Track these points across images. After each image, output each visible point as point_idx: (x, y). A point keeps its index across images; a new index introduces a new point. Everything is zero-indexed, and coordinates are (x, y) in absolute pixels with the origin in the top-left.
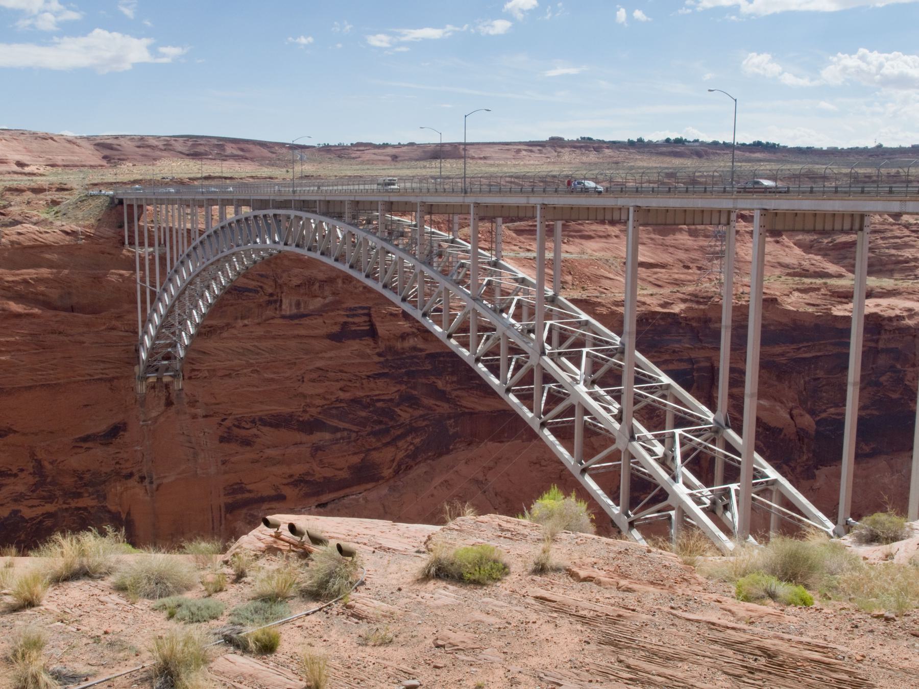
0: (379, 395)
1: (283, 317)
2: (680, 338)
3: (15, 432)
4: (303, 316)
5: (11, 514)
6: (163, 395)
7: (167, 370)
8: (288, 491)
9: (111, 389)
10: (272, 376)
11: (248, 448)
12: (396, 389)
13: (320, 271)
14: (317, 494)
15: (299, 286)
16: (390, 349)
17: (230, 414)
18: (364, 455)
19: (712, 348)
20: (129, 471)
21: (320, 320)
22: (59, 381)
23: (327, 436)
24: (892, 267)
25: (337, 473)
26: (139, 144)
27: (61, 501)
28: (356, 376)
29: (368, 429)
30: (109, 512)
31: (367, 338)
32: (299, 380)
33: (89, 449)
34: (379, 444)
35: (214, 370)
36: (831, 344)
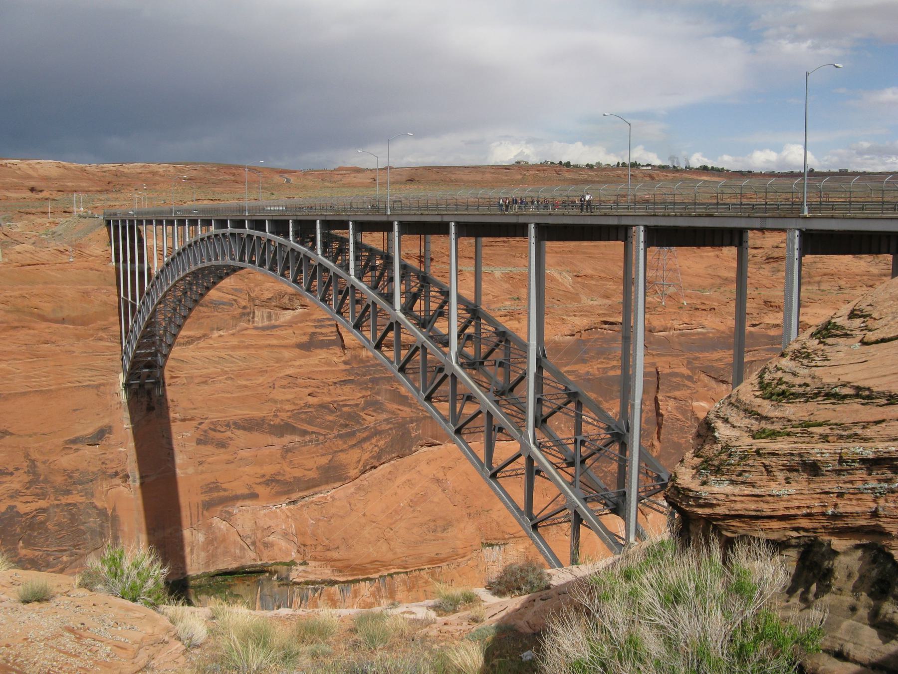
0: (345, 400)
1: (256, 328)
3: (11, 434)
4: (274, 327)
5: (7, 509)
6: (145, 400)
7: (149, 377)
8: (261, 490)
9: (98, 395)
10: (245, 383)
11: (223, 450)
12: (361, 395)
14: (288, 492)
15: (270, 299)
16: (355, 357)
17: (206, 418)
18: (331, 456)
19: (657, 355)
20: (114, 470)
21: (290, 331)
22: (52, 388)
23: (297, 439)
25: (307, 473)
27: (53, 498)
28: (324, 383)
29: (335, 432)
30: (95, 507)
31: (333, 347)
32: (270, 387)
33: (77, 450)
34: (345, 446)
35: (192, 377)
36: (764, 350)
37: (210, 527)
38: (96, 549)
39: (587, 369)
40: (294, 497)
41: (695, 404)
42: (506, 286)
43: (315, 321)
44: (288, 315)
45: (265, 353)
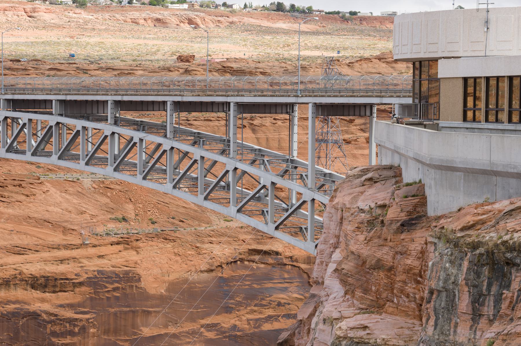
2: (286, 285)
39: (233, 322)
42: (104, 200)
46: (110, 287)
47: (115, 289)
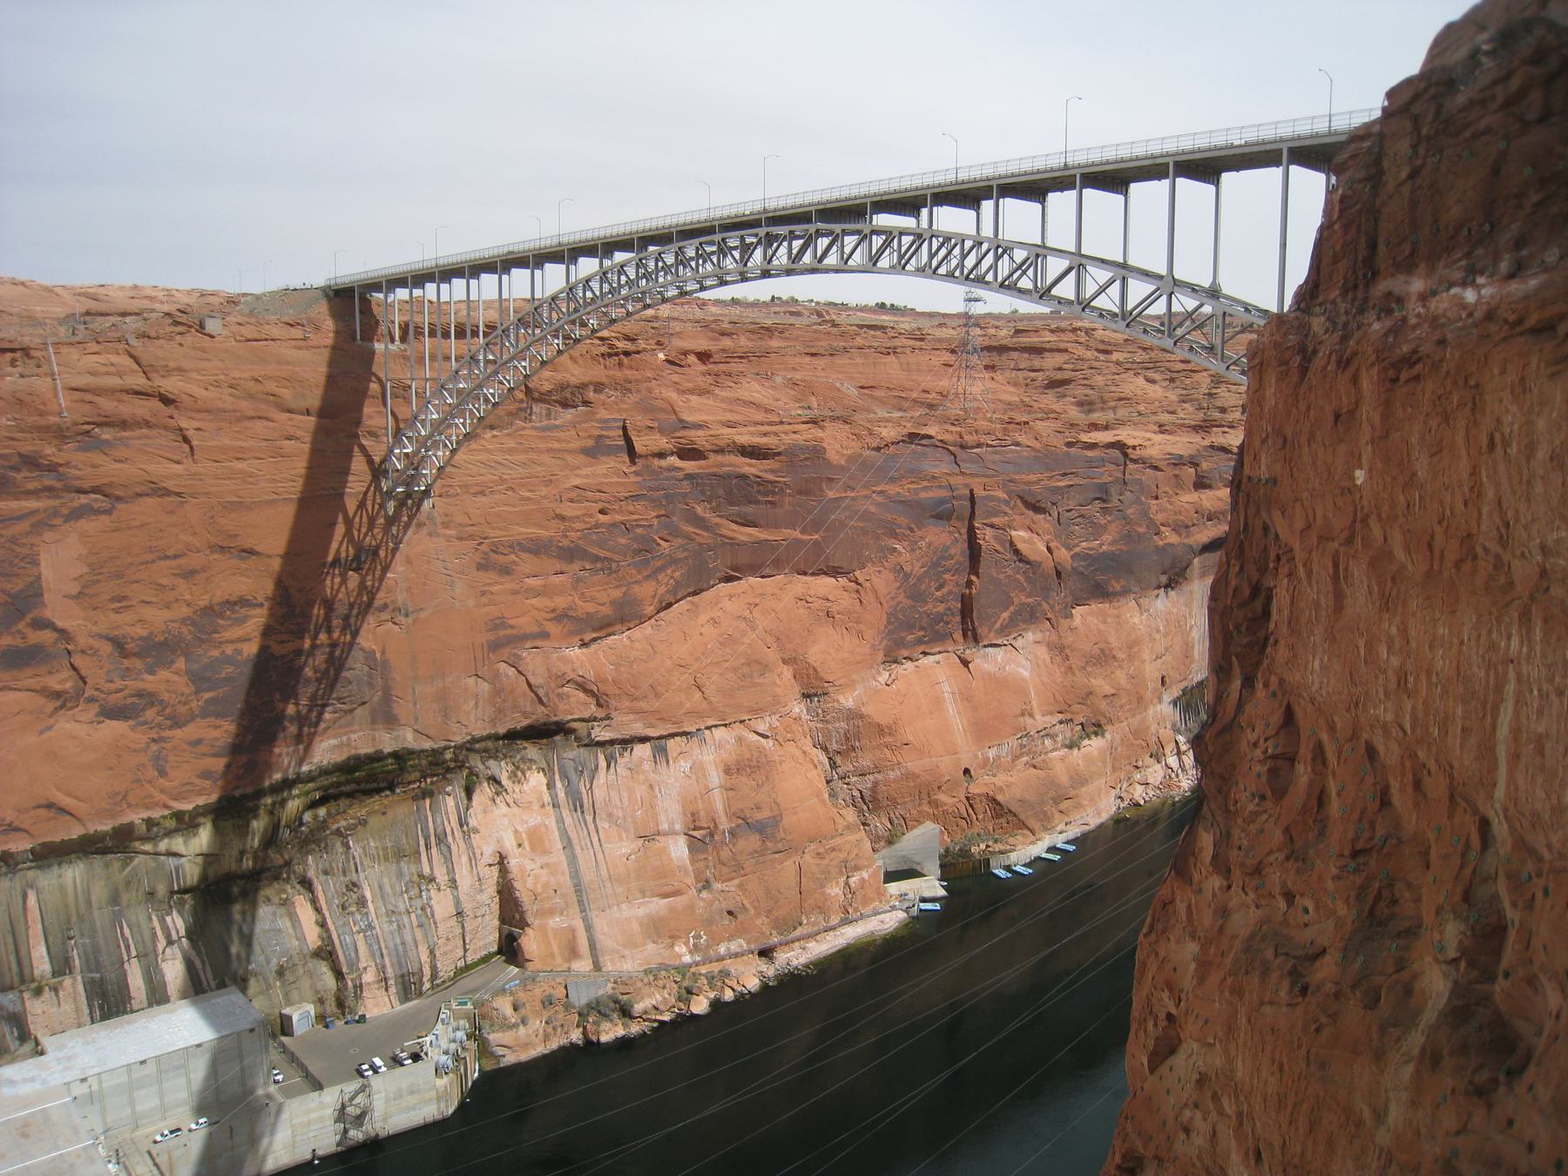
4: (557, 427)
8: (552, 628)
10: (528, 494)
11: (507, 578)
13: (573, 375)
14: (580, 632)
24: (1113, 404)
26: (132, 294)
35: (466, 486)
37: (497, 675)
38: (364, 703)
40: (588, 637)
41: (1013, 533)
42: (793, 392)
43: (599, 421)
44: (568, 415)
45: (546, 458)
46: (802, 457)
47: (806, 459)
